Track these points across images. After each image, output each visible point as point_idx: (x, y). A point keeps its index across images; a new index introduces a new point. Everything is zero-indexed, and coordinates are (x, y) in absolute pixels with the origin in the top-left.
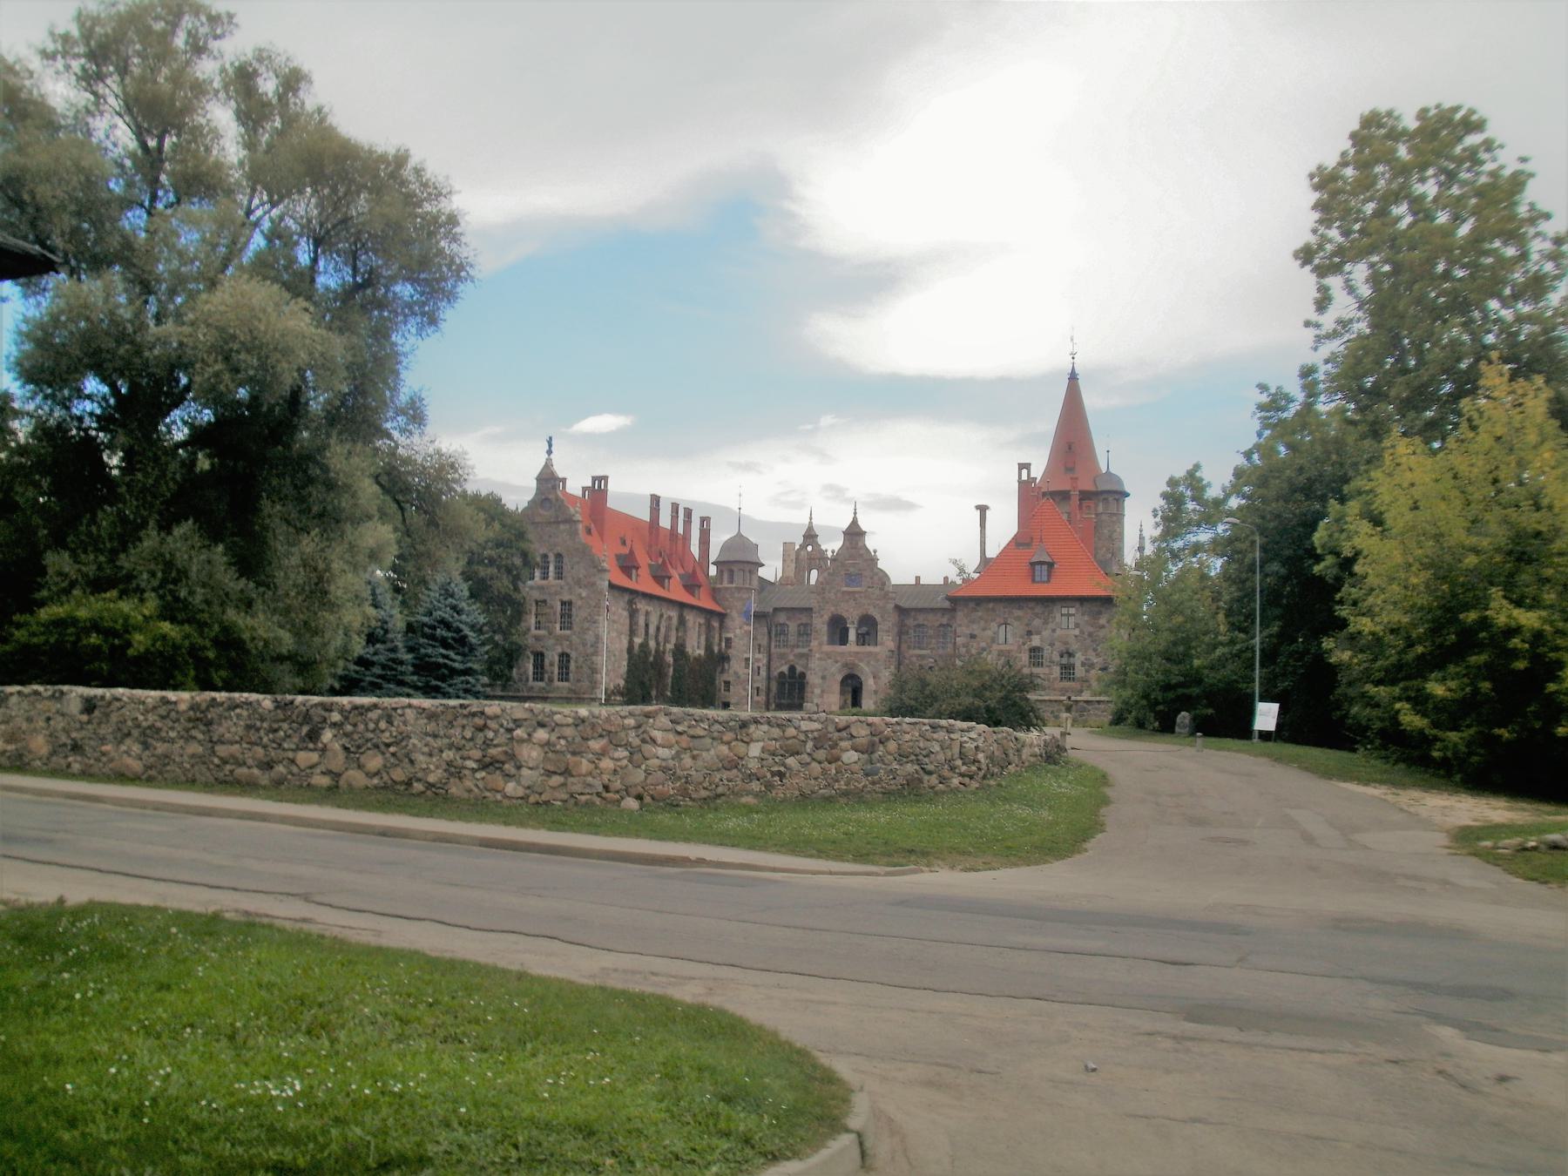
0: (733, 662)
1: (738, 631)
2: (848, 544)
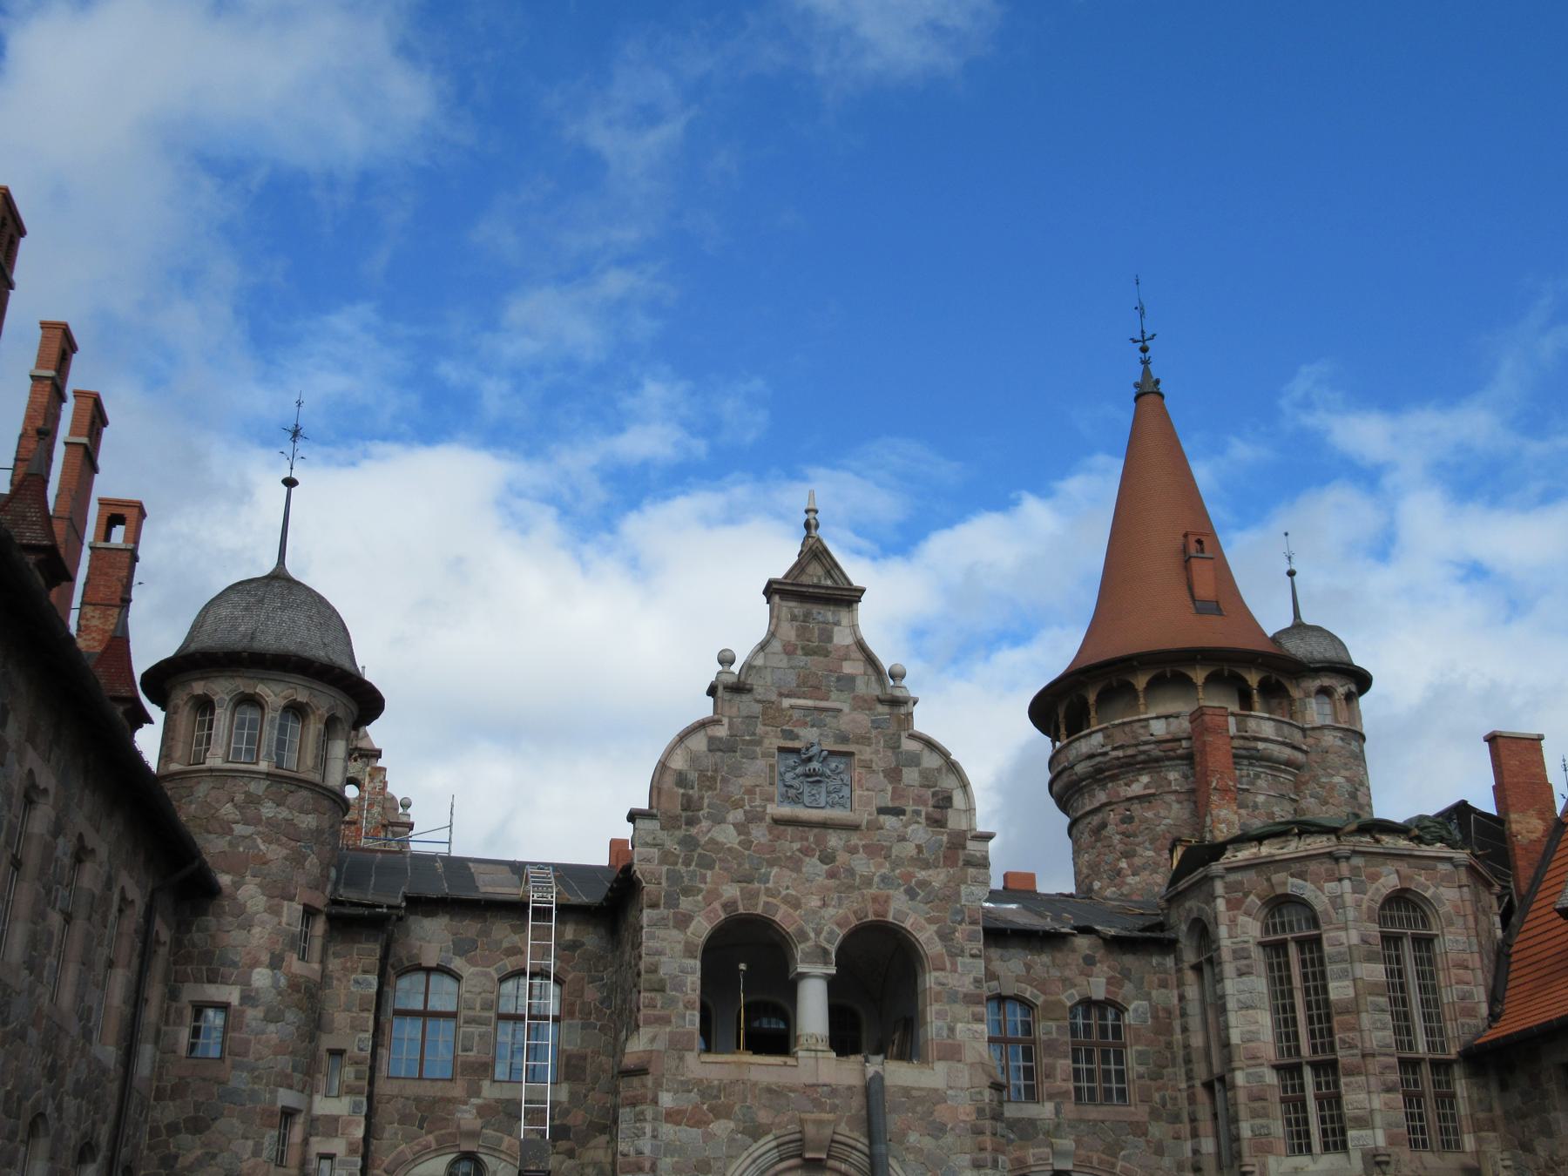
0: (230, 1123)
1: (261, 978)
2: (789, 632)
